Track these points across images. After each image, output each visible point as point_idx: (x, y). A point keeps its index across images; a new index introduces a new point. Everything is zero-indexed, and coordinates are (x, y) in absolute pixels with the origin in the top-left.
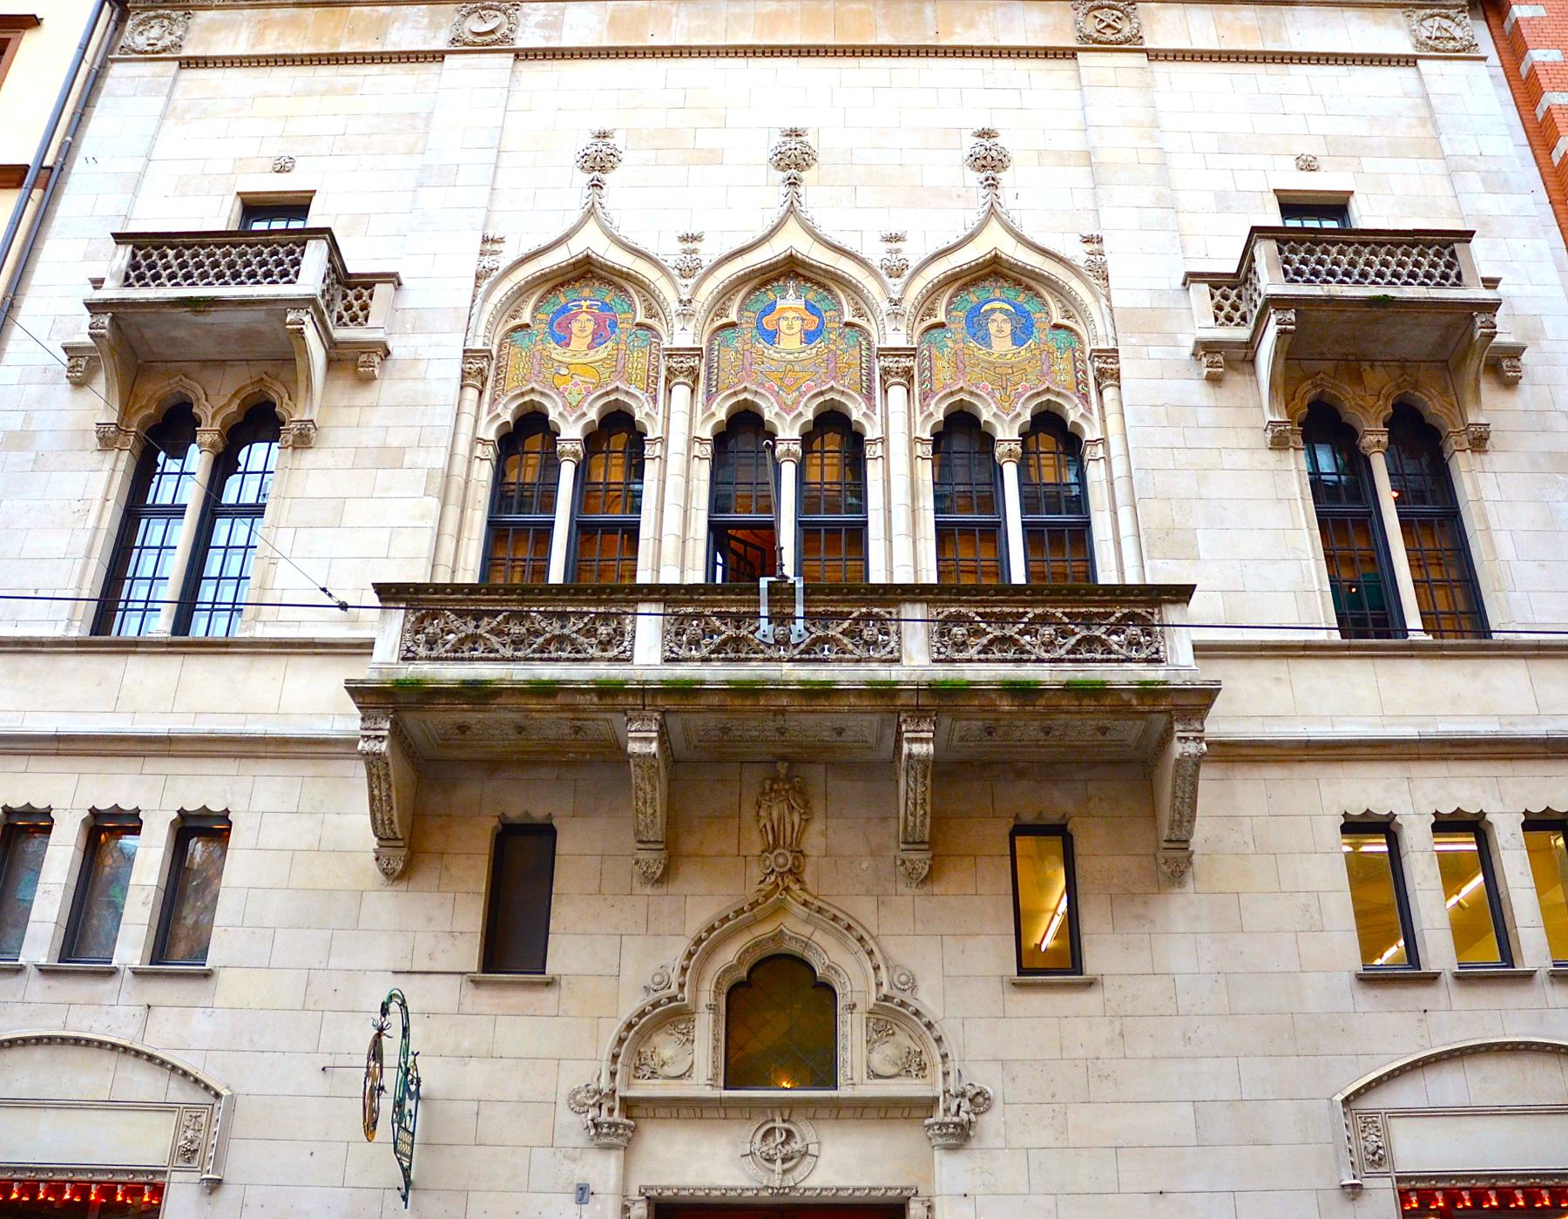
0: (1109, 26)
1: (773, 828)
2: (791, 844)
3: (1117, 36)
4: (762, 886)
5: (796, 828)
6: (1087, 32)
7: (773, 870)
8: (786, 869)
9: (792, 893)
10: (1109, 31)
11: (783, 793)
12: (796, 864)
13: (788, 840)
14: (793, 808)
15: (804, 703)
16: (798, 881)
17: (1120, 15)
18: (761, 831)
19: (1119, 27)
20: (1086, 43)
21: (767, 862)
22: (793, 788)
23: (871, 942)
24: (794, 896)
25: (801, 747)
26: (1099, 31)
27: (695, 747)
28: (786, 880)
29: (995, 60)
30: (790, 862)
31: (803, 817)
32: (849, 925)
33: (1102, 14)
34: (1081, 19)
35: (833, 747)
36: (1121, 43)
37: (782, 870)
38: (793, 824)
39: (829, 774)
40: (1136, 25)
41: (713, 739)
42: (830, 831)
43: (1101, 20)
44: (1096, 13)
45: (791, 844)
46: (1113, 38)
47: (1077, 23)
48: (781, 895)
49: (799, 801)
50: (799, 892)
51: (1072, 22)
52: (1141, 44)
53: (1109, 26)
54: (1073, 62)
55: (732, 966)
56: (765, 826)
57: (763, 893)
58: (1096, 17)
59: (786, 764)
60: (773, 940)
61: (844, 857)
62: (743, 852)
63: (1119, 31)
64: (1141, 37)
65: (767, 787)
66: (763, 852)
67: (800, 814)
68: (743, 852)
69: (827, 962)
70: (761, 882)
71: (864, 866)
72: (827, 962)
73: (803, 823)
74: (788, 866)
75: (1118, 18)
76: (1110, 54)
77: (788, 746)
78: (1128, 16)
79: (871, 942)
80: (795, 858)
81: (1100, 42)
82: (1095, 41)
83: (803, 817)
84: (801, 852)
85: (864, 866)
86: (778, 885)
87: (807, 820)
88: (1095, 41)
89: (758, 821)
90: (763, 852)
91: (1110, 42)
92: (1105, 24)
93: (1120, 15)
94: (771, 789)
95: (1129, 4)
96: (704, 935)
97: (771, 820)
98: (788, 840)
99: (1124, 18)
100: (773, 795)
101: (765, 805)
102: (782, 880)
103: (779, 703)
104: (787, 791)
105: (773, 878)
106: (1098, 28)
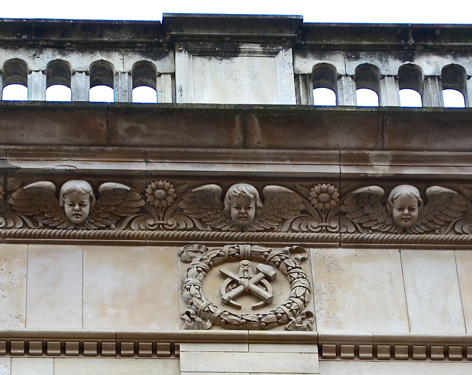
0: (248, 293)
3: (261, 312)
6: (202, 305)
10: (247, 304)
17: (271, 271)
19: (267, 295)
20: (200, 326)
26: (227, 303)
29: (15, 360)
33: (237, 271)
34: (192, 280)
36: (268, 326)
40: (300, 292)
43: (234, 282)
44: (225, 269)
46: (252, 316)
47: (184, 287)
51: (176, 286)
52: (309, 328)
53: (248, 293)
54: (171, 362)
58: (224, 276)
63: (267, 303)
64: (309, 315)
75: (267, 277)
76: (244, 347)
78: (287, 274)
81: (227, 325)
82: (217, 322)
88: (217, 322)
91: (247, 324)
92: (240, 289)
93: (271, 271)
95: (293, 252)
99: (281, 277)
106: (226, 297)
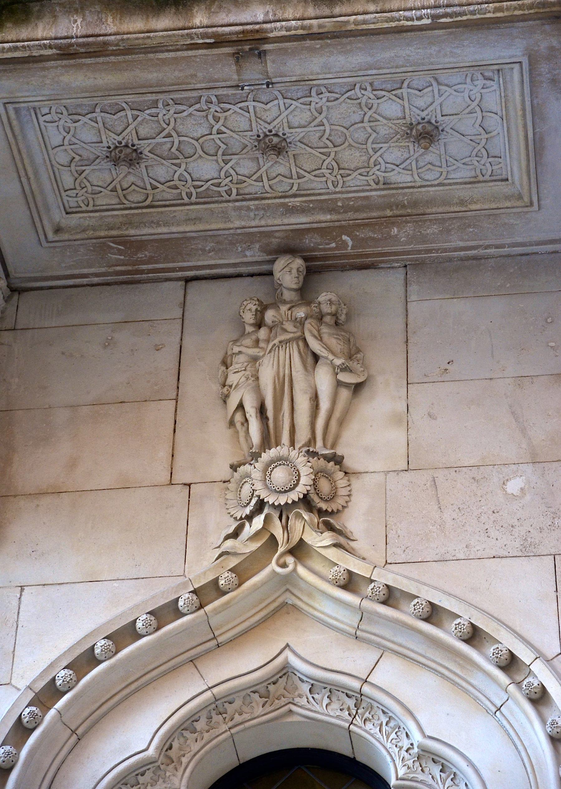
1: (262, 410)
2: (312, 440)
4: (230, 543)
5: (325, 405)
7: (261, 505)
8: (294, 496)
9: (310, 563)
11: (289, 326)
12: (324, 486)
13: (303, 436)
14: (316, 358)
15: (311, 11)
16: (330, 527)
18: (232, 423)
21: (246, 490)
22: (320, 318)
23: (538, 668)
24: (318, 566)
25: (331, 211)
27: (58, 230)
28: (296, 526)
30: (305, 480)
31: (344, 377)
32: (474, 628)
35: (415, 204)
37: (282, 500)
38: (315, 399)
39: (413, 288)
41: (102, 201)
42: (417, 415)
45: (312, 440)
48: (284, 566)
49: (333, 342)
50: (333, 554)
55: (150, 762)
56: (241, 406)
57: (233, 562)
59: (298, 263)
60: (266, 696)
61: (458, 468)
62: (181, 477)
65: (249, 317)
66: (234, 468)
67: (336, 370)
68: (179, 478)
69: (417, 737)
70: (235, 535)
71: (514, 486)
72: (417, 737)
73: (345, 394)
74: (301, 490)
77: (302, 210)
79: (538, 668)
80: (318, 474)
83: (344, 377)
84: (338, 460)
85: (514, 486)
86: (273, 538)
87: (357, 388)
89: (225, 399)
90: (234, 468)
94: (259, 324)
96: (62, 676)
97: (258, 390)
98: (303, 436)
100: (263, 333)
101: (239, 362)
102: (286, 528)
103: (245, 16)
104: (300, 323)
105: (258, 522)
